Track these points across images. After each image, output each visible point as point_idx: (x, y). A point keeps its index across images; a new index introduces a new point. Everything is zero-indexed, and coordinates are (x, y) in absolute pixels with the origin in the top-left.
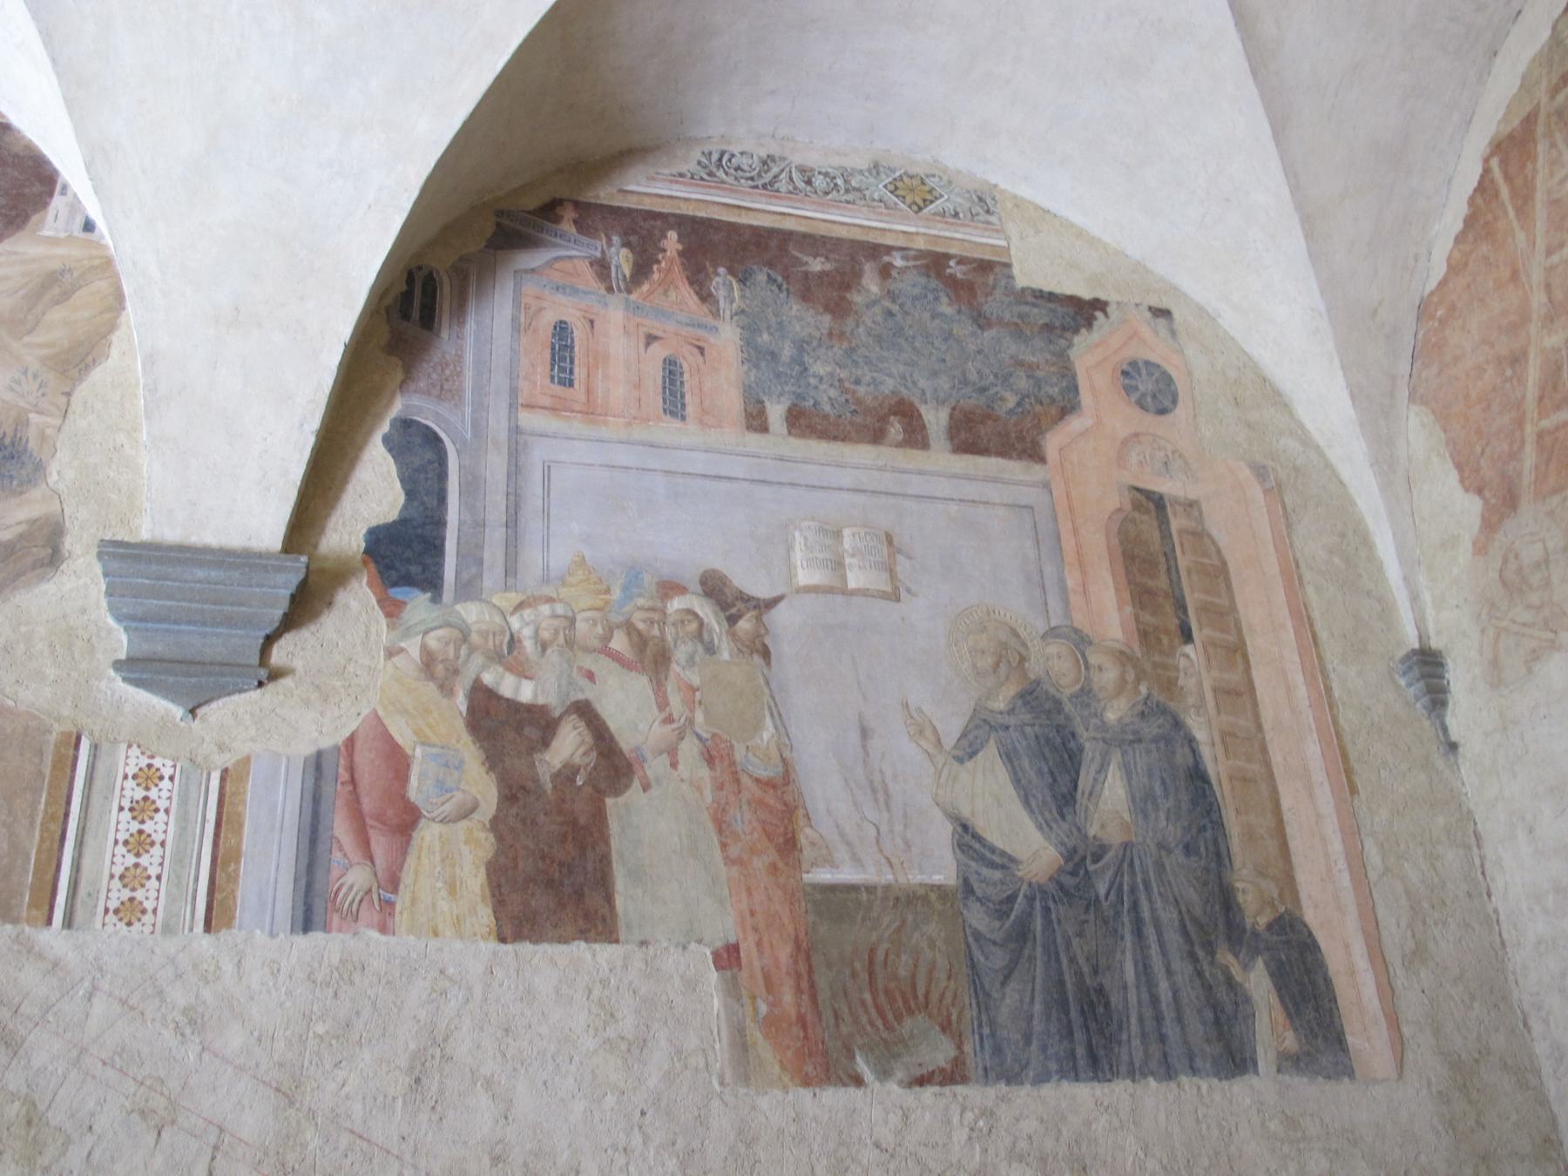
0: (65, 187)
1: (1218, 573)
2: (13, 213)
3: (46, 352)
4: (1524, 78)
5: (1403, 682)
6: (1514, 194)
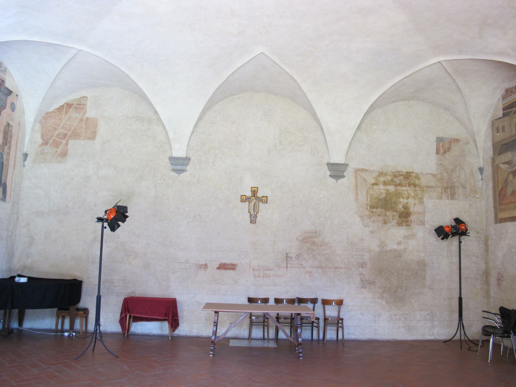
1: (11, 137)
4: (74, 99)
5: (22, 156)
6: (66, 111)
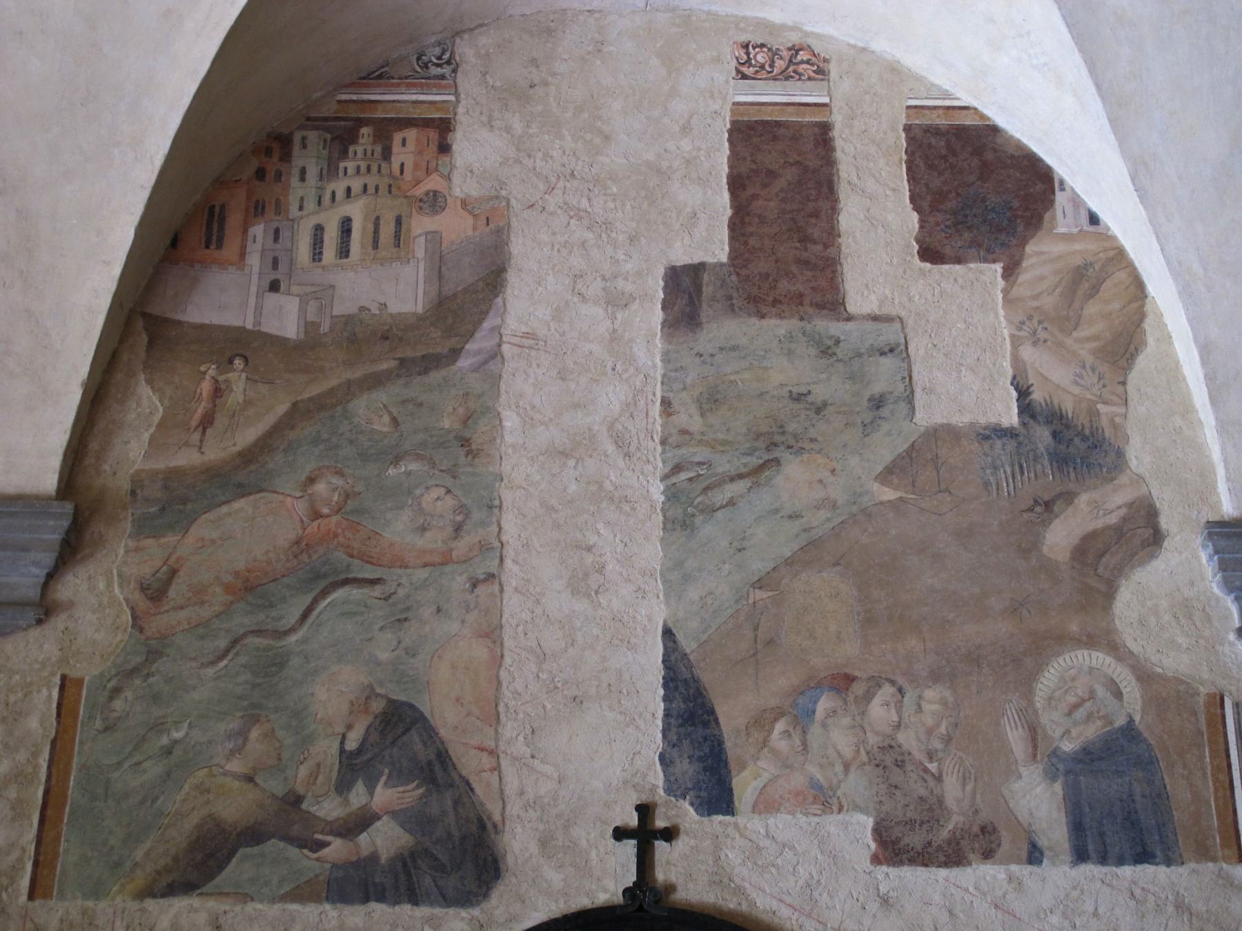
0: (1062, 182)
2: (1028, 214)
3: (1094, 345)
